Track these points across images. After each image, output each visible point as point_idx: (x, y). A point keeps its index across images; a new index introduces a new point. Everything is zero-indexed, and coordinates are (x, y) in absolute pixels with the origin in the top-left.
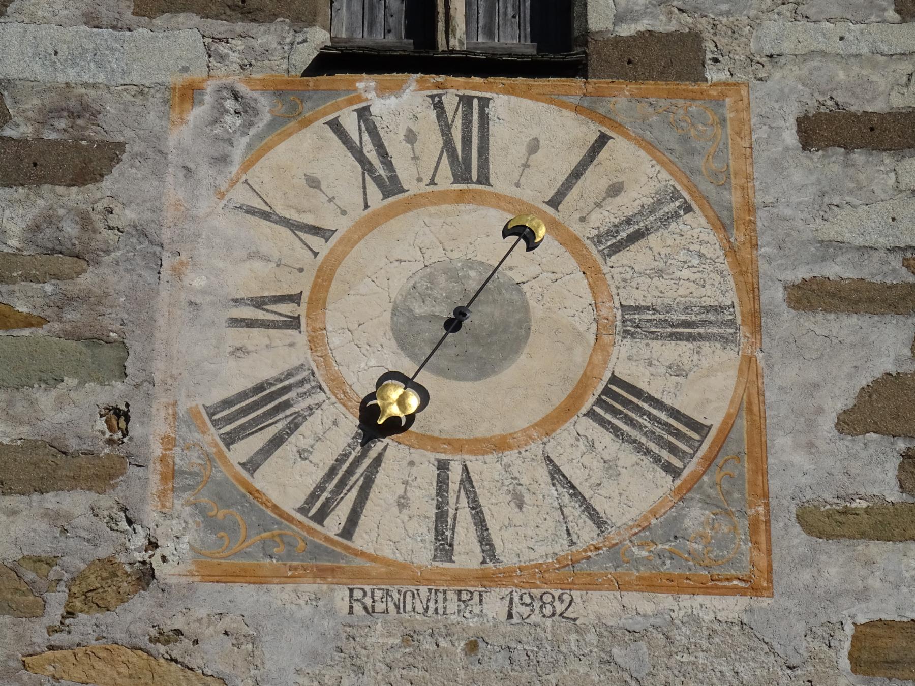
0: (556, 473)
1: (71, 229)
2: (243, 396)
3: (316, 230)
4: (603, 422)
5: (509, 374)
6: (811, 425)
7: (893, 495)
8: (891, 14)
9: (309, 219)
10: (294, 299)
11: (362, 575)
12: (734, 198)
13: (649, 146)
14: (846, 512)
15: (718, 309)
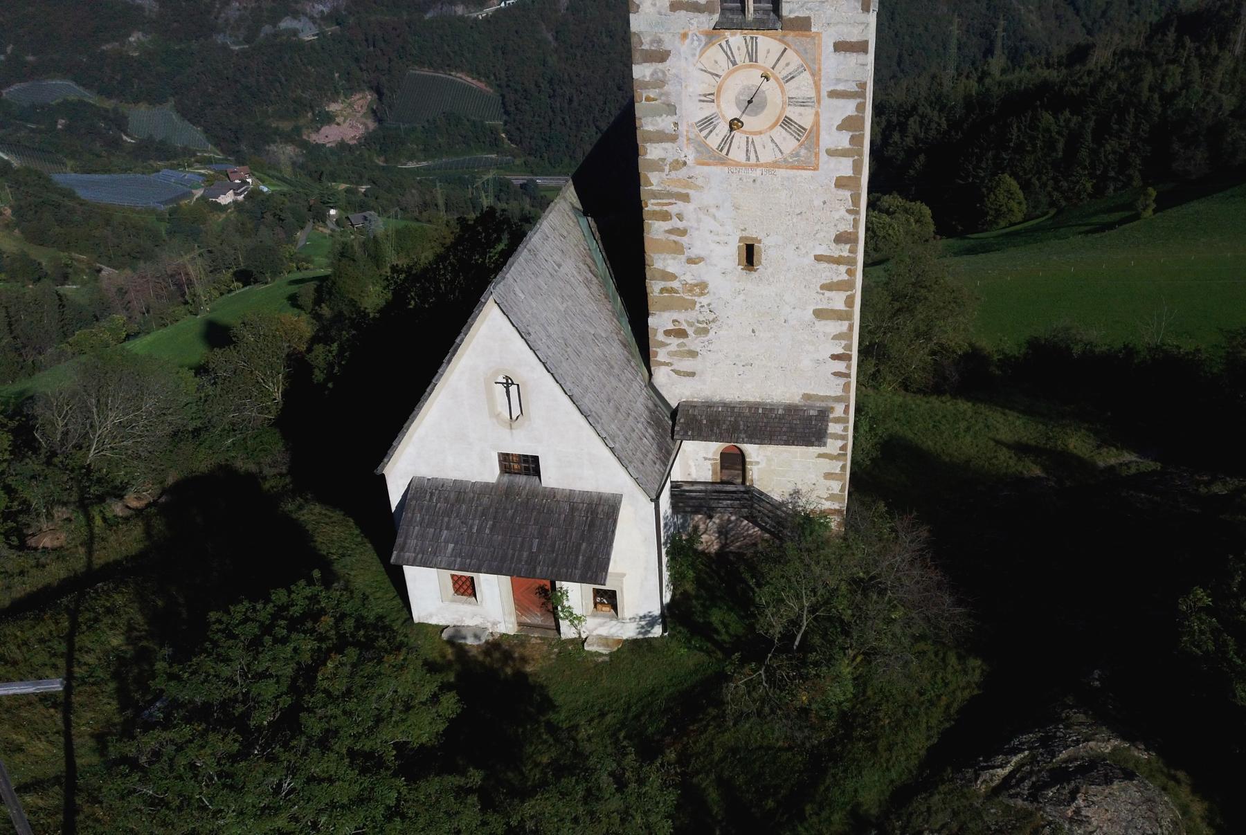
0: (772, 140)
1: (660, 75)
2: (703, 120)
3: (717, 75)
4: (783, 128)
8: (860, 11)
13: (796, 52)
14: (837, 150)
15: (810, 98)
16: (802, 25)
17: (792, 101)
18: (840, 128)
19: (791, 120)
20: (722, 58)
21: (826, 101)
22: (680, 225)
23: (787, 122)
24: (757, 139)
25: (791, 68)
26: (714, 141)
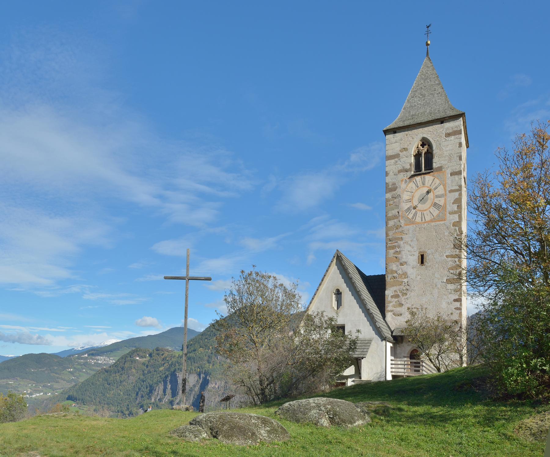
0: (430, 212)
3: (412, 192)
5: (426, 204)
6: (450, 204)
7: (456, 209)
8: (459, 160)
9: (411, 191)
10: (410, 199)
11: (416, 224)
12: (444, 183)
13: (438, 179)
16: (440, 169)
17: (437, 196)
18: (453, 203)
19: (436, 203)
20: (414, 186)
22: (398, 250)
23: (435, 205)
24: (425, 212)
25: (436, 185)
26: (410, 216)
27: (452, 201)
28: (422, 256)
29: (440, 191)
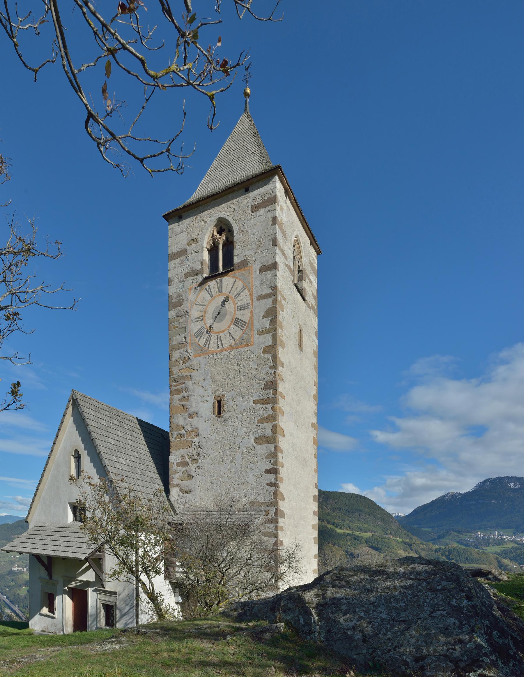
0: (230, 333)
3: (204, 305)
7: (268, 326)
10: (202, 316)
11: (210, 353)
18: (264, 317)
19: (238, 319)
21: (256, 303)
23: (237, 322)
25: (238, 290)
26: (202, 342)
27: (262, 314)
28: (219, 402)
29: (244, 299)
